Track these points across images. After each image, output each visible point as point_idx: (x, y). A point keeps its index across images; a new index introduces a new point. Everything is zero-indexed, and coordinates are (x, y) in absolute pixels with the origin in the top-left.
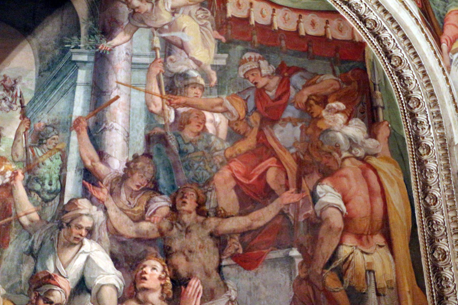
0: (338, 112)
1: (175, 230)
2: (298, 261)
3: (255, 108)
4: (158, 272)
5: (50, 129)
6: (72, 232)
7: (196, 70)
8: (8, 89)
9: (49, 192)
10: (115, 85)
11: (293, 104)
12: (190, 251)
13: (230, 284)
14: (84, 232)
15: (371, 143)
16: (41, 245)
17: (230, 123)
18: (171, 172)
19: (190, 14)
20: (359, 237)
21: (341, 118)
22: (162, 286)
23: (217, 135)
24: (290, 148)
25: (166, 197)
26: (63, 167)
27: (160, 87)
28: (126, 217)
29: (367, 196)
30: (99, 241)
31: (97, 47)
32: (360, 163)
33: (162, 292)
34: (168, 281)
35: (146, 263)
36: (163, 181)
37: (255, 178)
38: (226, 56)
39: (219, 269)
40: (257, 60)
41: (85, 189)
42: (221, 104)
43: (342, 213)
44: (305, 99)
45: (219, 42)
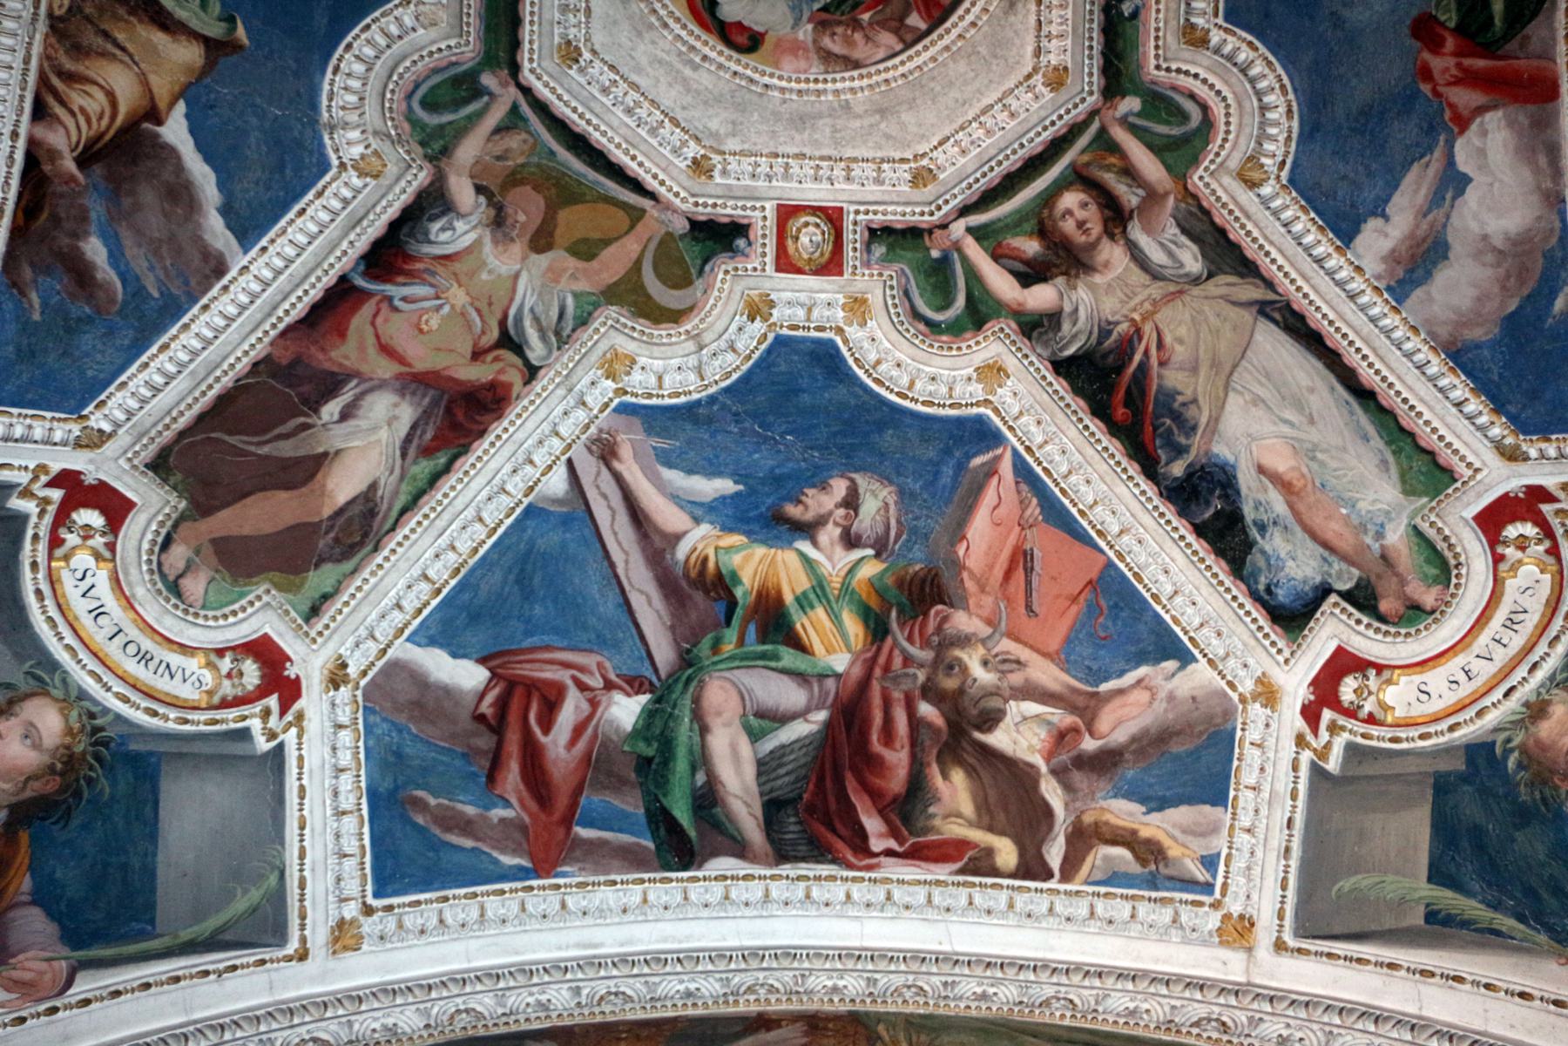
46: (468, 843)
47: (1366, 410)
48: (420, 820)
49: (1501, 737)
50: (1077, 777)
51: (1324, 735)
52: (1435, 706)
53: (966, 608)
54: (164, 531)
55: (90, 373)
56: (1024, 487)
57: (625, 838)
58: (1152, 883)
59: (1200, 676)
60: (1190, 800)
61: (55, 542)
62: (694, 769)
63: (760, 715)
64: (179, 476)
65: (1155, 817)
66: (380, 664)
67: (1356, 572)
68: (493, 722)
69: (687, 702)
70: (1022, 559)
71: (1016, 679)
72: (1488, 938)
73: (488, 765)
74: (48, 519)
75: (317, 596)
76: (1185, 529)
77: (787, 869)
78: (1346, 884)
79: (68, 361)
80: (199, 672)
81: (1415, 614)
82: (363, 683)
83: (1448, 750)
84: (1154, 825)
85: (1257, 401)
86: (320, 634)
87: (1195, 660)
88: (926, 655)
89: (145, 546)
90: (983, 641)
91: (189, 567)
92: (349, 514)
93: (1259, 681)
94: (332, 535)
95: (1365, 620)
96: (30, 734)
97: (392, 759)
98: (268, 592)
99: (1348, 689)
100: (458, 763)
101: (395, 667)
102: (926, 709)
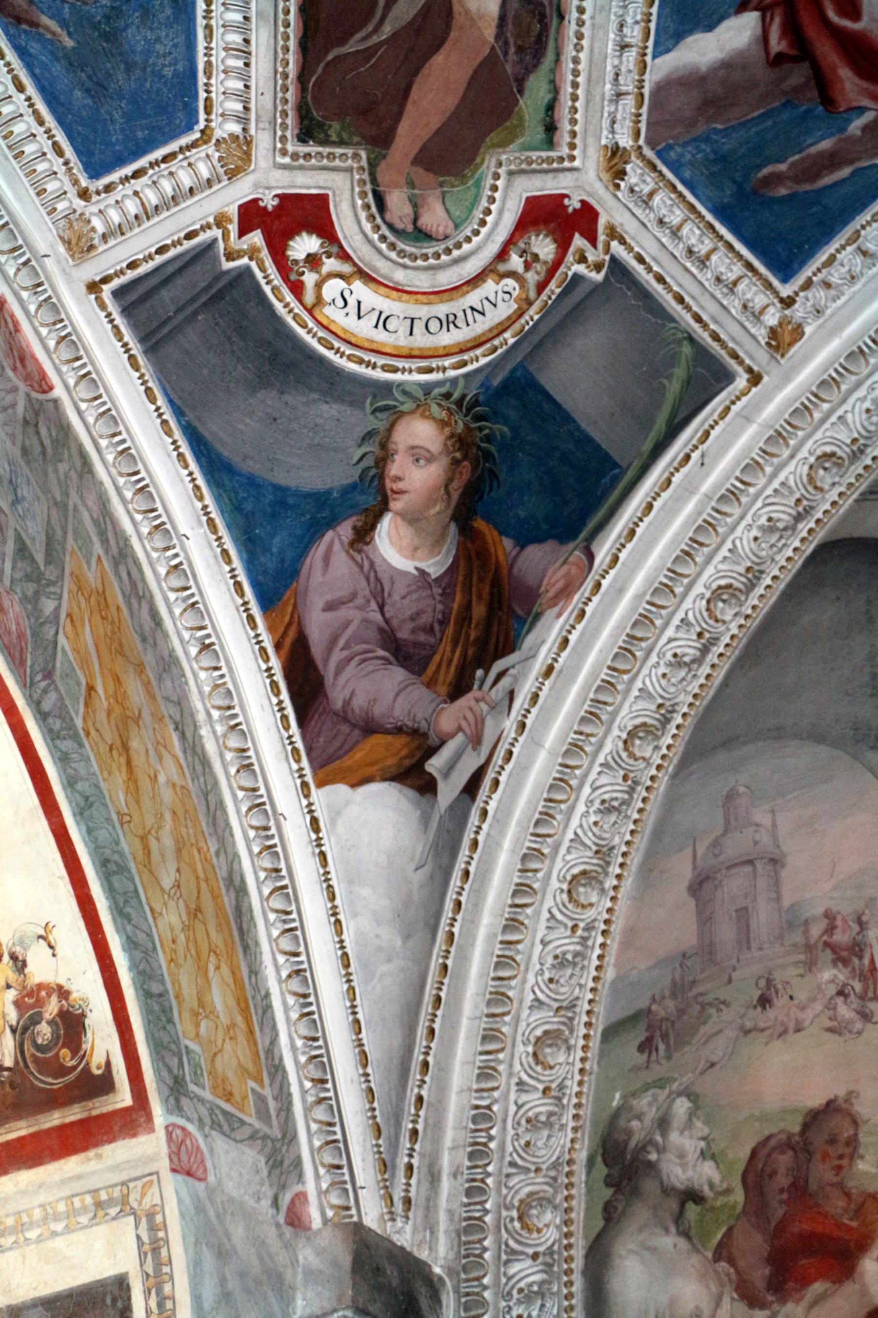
8: (844, 954)
46: (845, 172)
48: (783, 191)
54: (370, 198)
55: (168, 72)
61: (297, 289)
64: (336, 126)
66: (644, 110)
68: (793, 52)
73: (815, 93)
74: (269, 263)
75: (542, 114)
79: (138, 72)
80: (499, 288)
82: (641, 142)
86: (572, 146)
89: (367, 227)
91: (416, 205)
92: (511, 14)
94: (512, 50)
96: (418, 455)
97: (715, 169)
98: (500, 164)
100: (785, 116)
101: (660, 89)
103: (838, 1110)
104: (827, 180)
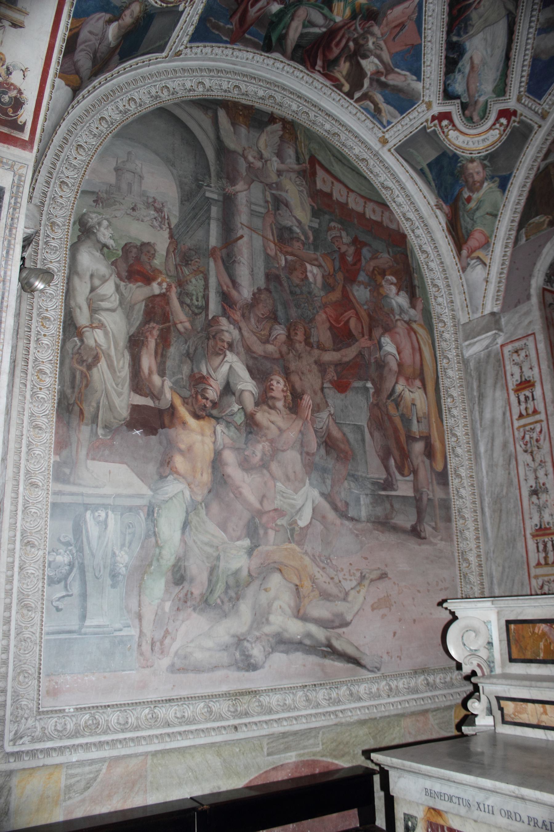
0: (392, 284)
1: (291, 355)
2: (372, 391)
3: (340, 268)
4: (281, 386)
5: (193, 253)
6: (217, 343)
7: (298, 227)
9: (197, 307)
10: (240, 225)
11: (364, 270)
12: (303, 373)
13: (330, 402)
14: (226, 345)
15: (412, 312)
16: (195, 351)
17: (323, 276)
18: (286, 308)
19: (290, 179)
20: (407, 379)
21: (394, 289)
22: (285, 397)
23: (315, 284)
24: (364, 305)
25: (283, 326)
26: (206, 287)
27: (273, 235)
28: (255, 338)
29: (411, 351)
30: (238, 354)
31: (224, 190)
32: (406, 326)
33: (285, 402)
34: (289, 394)
35: (273, 377)
36: (281, 313)
37: (342, 323)
38: (318, 221)
39: (322, 389)
40: (339, 230)
41: (224, 309)
42: (316, 260)
43: (397, 360)
44: (371, 269)
45: (313, 208)
46: (217, 32)
47: (505, 62)
49: (462, 159)
50: (375, 84)
51: (432, 125)
52: (456, 142)
53: (379, 27)
56: (417, 9)
57: (256, 40)
58: (373, 116)
59: (419, 86)
60: (395, 107)
62: (284, 28)
63: (309, 22)
65: (385, 105)
67: (468, 100)
69: (292, 11)
70: (402, 26)
71: (378, 52)
72: (428, 183)
76: (443, 55)
77: (292, 63)
78: (411, 150)
81: (470, 119)
83: (452, 151)
84: (383, 106)
85: (486, 40)
87: (420, 81)
88: (360, 31)
90: (377, 38)
93: (429, 101)
95: (460, 112)
99: (445, 123)
102: (351, 44)
103: (151, 245)
104: (214, 31)
